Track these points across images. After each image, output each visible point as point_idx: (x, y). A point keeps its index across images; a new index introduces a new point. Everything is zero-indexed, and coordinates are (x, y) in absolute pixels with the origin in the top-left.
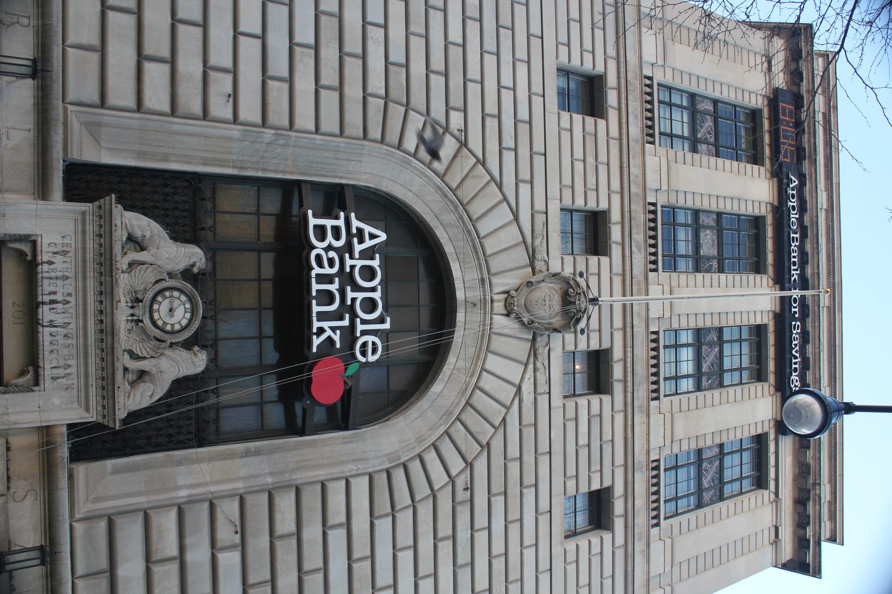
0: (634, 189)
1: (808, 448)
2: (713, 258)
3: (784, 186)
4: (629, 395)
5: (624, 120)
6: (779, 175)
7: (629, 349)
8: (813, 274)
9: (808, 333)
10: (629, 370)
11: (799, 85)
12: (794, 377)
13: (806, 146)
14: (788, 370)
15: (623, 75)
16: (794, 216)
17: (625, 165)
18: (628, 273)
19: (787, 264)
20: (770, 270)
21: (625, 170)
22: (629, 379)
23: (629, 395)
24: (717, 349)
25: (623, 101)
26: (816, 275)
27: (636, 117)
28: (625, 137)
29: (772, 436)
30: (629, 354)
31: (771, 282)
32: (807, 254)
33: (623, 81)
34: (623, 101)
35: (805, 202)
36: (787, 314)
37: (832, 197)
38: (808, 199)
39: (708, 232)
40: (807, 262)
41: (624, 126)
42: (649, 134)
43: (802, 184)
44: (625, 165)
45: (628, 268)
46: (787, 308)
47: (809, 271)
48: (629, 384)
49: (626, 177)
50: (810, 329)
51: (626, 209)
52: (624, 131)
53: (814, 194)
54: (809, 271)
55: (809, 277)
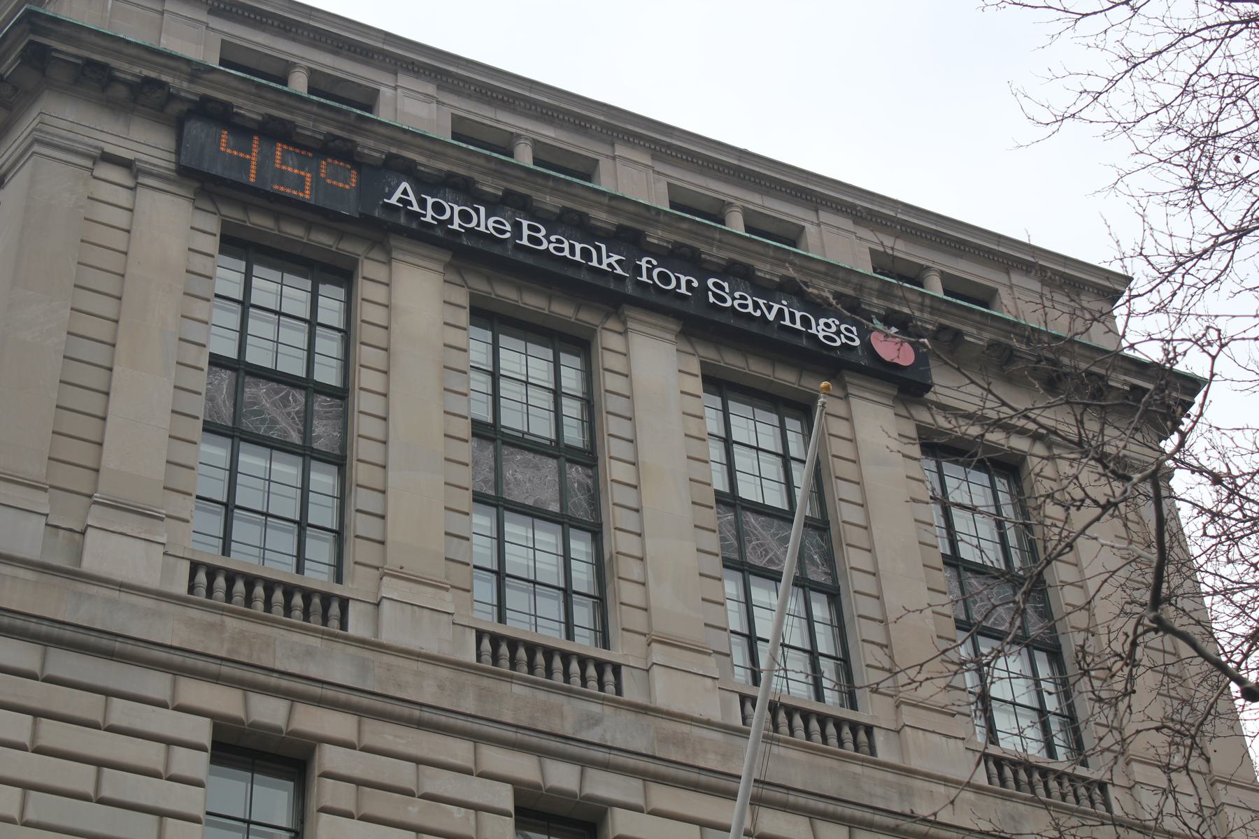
0: (469, 706)
1: (958, 334)
2: (561, 473)
3: (414, 226)
4: (878, 818)
5: (317, 690)
6: (391, 232)
7: (792, 798)
8: (612, 210)
9: (732, 263)
10: (831, 807)
11: (172, 97)
12: (820, 329)
13: (325, 128)
14: (804, 342)
15: (213, 667)
16: (484, 222)
17: (416, 713)
18: (642, 764)
19: (584, 276)
20: (587, 317)
21: (427, 715)
22: (848, 811)
23: (878, 818)
24: (751, 518)
25: (273, 680)
26: (614, 203)
27: (309, 653)
28: (355, 699)
29: (924, 416)
30: (802, 800)
31: (612, 324)
32: (565, 210)
33: (226, 669)
34: (273, 680)
35: (451, 175)
36: (691, 309)
37: (413, 62)
38: (445, 167)
39: (508, 474)
40: (583, 216)
41: (330, 693)
42: (323, 609)
43: (409, 171)
44: (416, 713)
45: (631, 762)
46: (677, 305)
47: (603, 216)
48: (858, 813)
49: (443, 719)
50: (725, 254)
51: (509, 734)
52: (343, 696)
53: (437, 148)
54: (603, 216)
55: (615, 220)
